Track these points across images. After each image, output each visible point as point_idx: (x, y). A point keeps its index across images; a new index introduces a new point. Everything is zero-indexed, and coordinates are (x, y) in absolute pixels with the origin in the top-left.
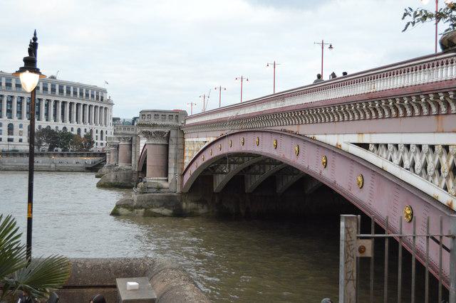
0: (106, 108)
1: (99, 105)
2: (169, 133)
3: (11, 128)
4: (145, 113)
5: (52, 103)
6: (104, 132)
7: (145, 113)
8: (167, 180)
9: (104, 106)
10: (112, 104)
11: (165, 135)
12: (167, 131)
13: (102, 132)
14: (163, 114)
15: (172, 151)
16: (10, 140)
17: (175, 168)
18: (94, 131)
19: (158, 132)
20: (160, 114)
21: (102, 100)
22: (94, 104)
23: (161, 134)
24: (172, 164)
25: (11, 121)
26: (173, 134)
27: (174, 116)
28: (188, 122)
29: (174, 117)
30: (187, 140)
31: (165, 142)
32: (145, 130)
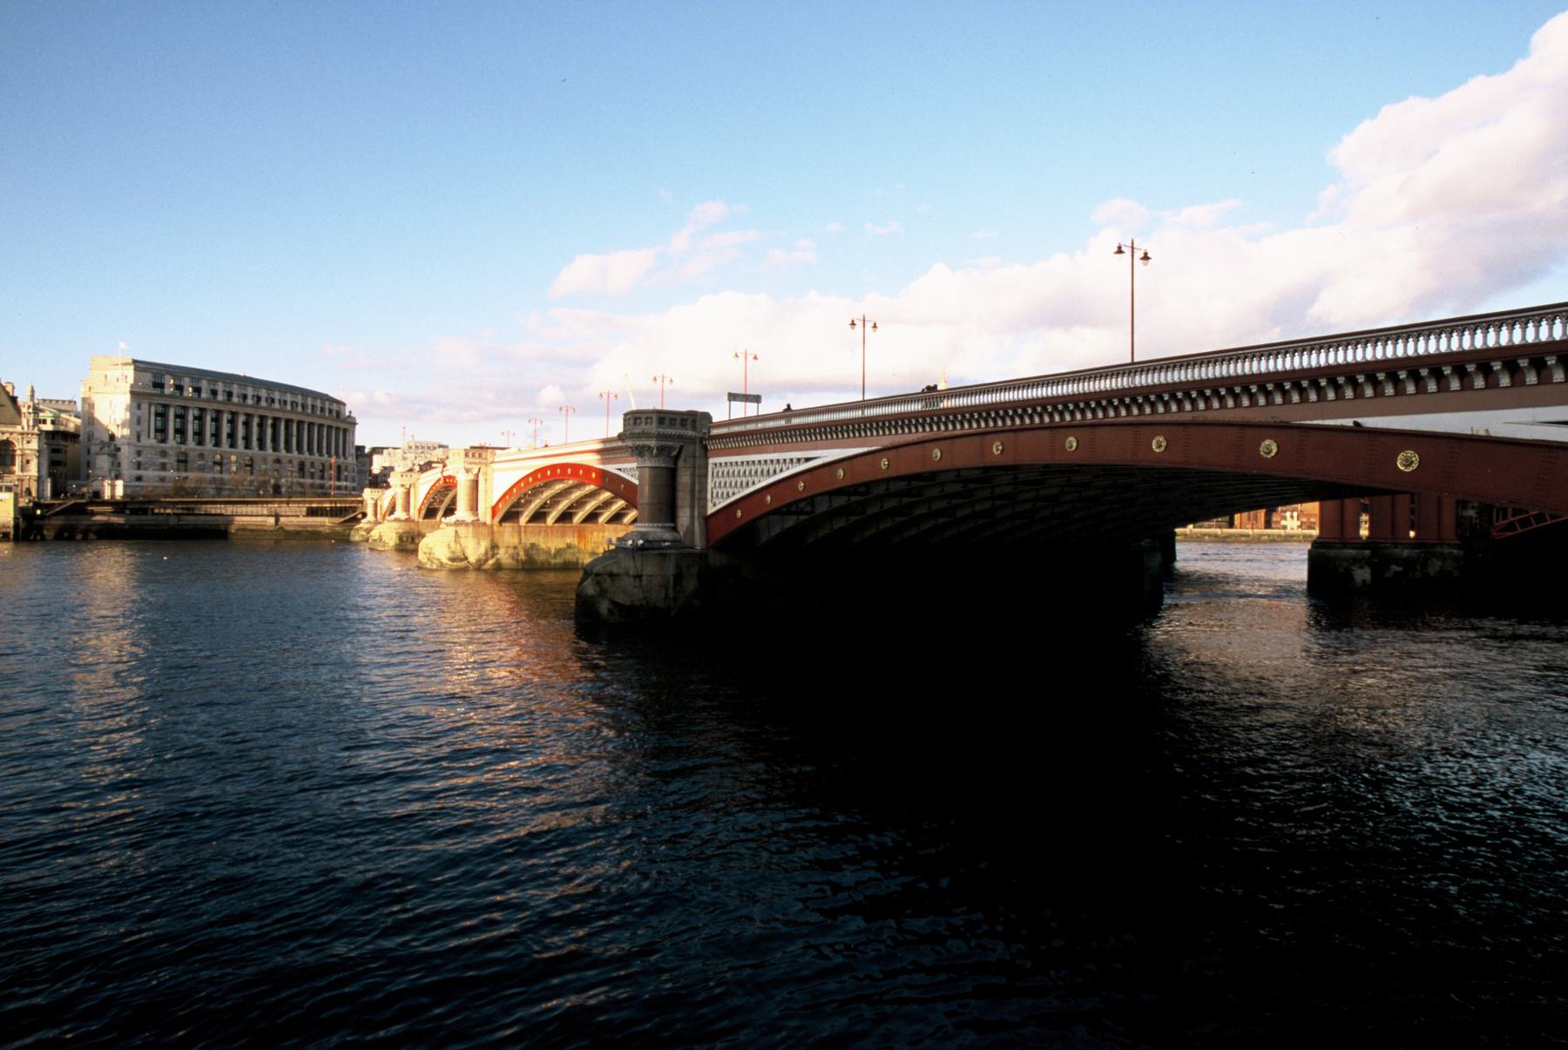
0: (345, 430)
1: (335, 424)
4: (641, 415)
5: (256, 421)
6: (343, 467)
7: (641, 415)
8: (675, 529)
9: (342, 426)
11: (674, 453)
13: (339, 467)
14: (673, 416)
15: (684, 478)
17: (692, 508)
22: (327, 422)
23: (671, 449)
24: (683, 498)
27: (643, 420)
28: (714, 432)
29: (689, 422)
30: (711, 461)
31: (671, 465)
32: (641, 443)
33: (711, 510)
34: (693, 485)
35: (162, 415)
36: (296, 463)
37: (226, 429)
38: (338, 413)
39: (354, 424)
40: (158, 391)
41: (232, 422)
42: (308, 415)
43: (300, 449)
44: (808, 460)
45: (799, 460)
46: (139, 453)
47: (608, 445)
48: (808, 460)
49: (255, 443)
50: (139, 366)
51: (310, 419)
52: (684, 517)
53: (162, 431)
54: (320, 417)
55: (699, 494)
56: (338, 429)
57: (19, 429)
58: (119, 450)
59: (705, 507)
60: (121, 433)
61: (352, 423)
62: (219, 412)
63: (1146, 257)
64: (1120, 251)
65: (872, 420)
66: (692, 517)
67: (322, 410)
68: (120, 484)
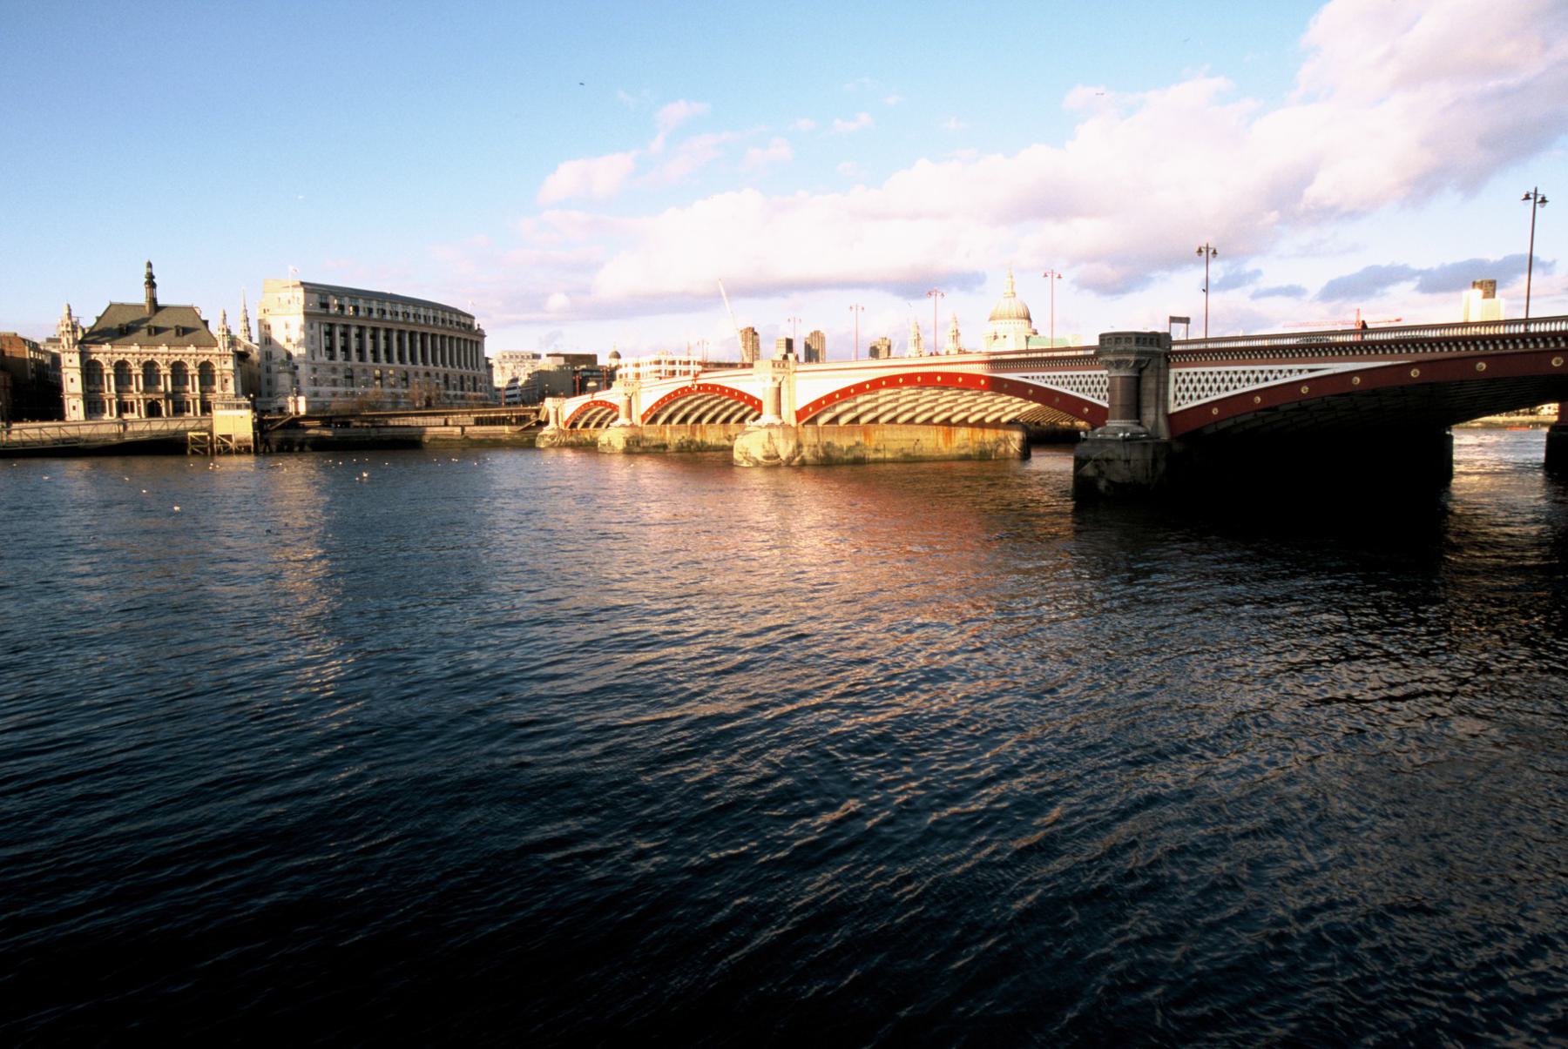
0: (477, 343)
1: (469, 337)
9: (475, 339)
15: (1150, 384)
24: (1148, 399)
28: (1175, 348)
30: (1173, 372)
33: (1173, 408)
34: (1158, 389)
35: (330, 334)
36: (441, 375)
37: (354, 345)
38: (471, 326)
39: (483, 336)
40: (323, 311)
41: (345, 335)
42: (421, 325)
43: (434, 362)
44: (1311, 371)
45: (1300, 371)
46: (314, 370)
47: (992, 358)
48: (1311, 371)
49: (369, 355)
50: (309, 288)
52: (1149, 415)
53: (331, 348)
54: (441, 328)
55: (1161, 398)
56: (472, 341)
57: (216, 350)
58: (296, 368)
59: (1166, 406)
60: (298, 351)
61: (481, 335)
62: (347, 327)
63: (1544, 201)
64: (1527, 197)
66: (1157, 415)
67: (435, 318)
68: (302, 400)
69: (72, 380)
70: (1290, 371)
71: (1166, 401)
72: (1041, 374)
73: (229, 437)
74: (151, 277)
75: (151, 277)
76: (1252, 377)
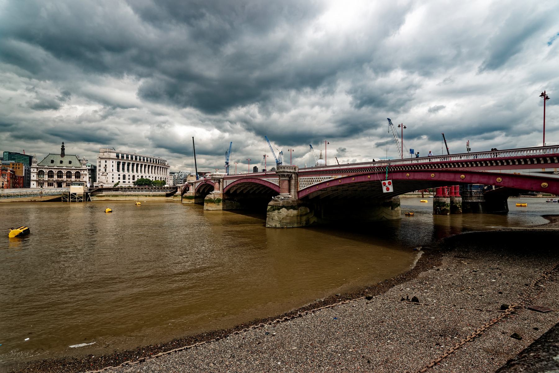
0: (167, 168)
1: (164, 167)
2: (292, 175)
3: (124, 177)
9: (166, 167)
10: (169, 167)
12: (290, 174)
15: (293, 182)
16: (124, 182)
18: (162, 178)
19: (287, 175)
20: (289, 167)
21: (165, 164)
24: (293, 187)
25: (124, 173)
26: (293, 175)
33: (299, 190)
35: (119, 164)
36: (154, 177)
44: (329, 178)
45: (327, 178)
48: (329, 178)
51: (158, 165)
52: (293, 191)
65: (342, 170)
69: (34, 176)
70: (325, 178)
71: (298, 187)
72: (271, 179)
73: (75, 194)
74: (63, 146)
75: (63, 146)
76: (316, 180)
